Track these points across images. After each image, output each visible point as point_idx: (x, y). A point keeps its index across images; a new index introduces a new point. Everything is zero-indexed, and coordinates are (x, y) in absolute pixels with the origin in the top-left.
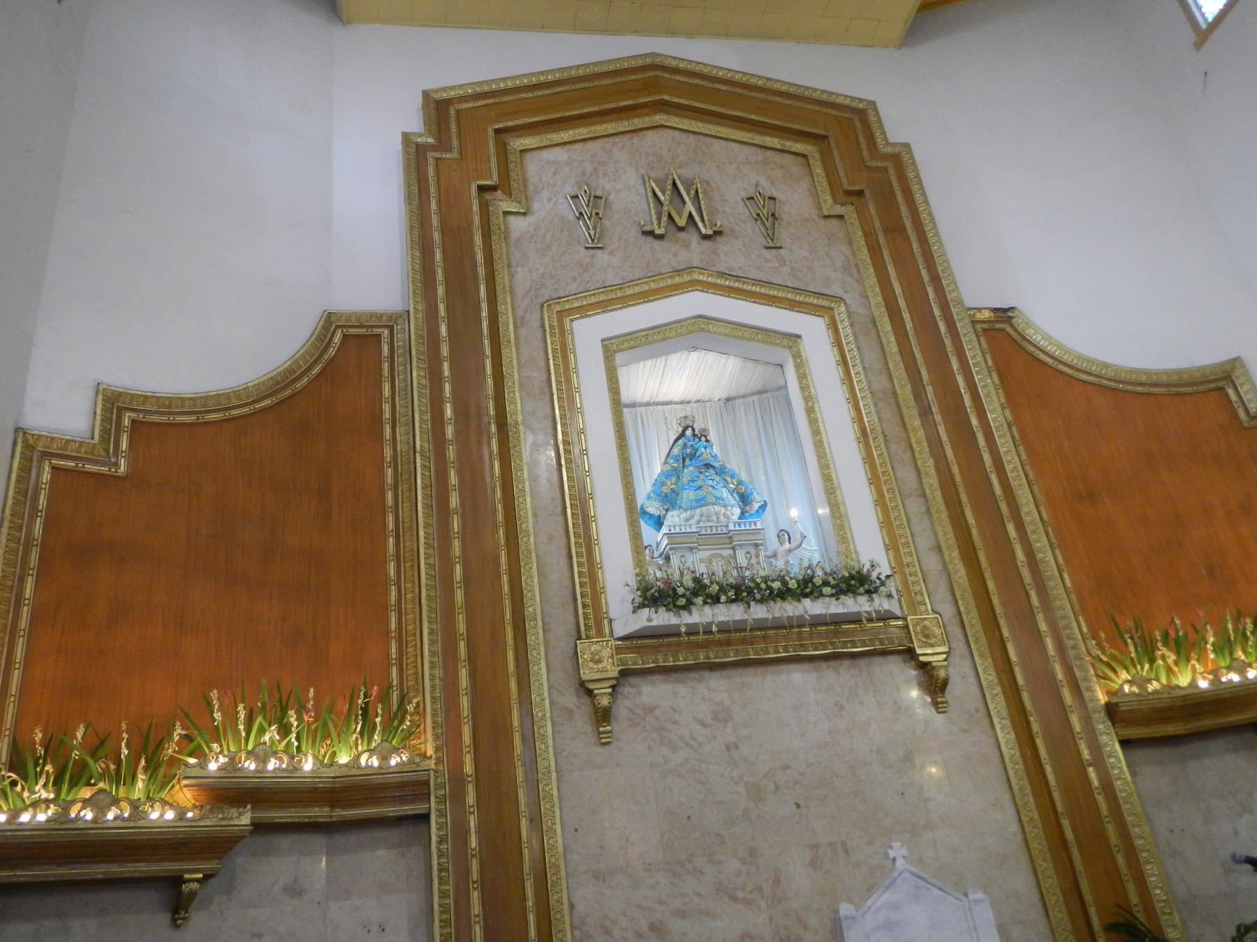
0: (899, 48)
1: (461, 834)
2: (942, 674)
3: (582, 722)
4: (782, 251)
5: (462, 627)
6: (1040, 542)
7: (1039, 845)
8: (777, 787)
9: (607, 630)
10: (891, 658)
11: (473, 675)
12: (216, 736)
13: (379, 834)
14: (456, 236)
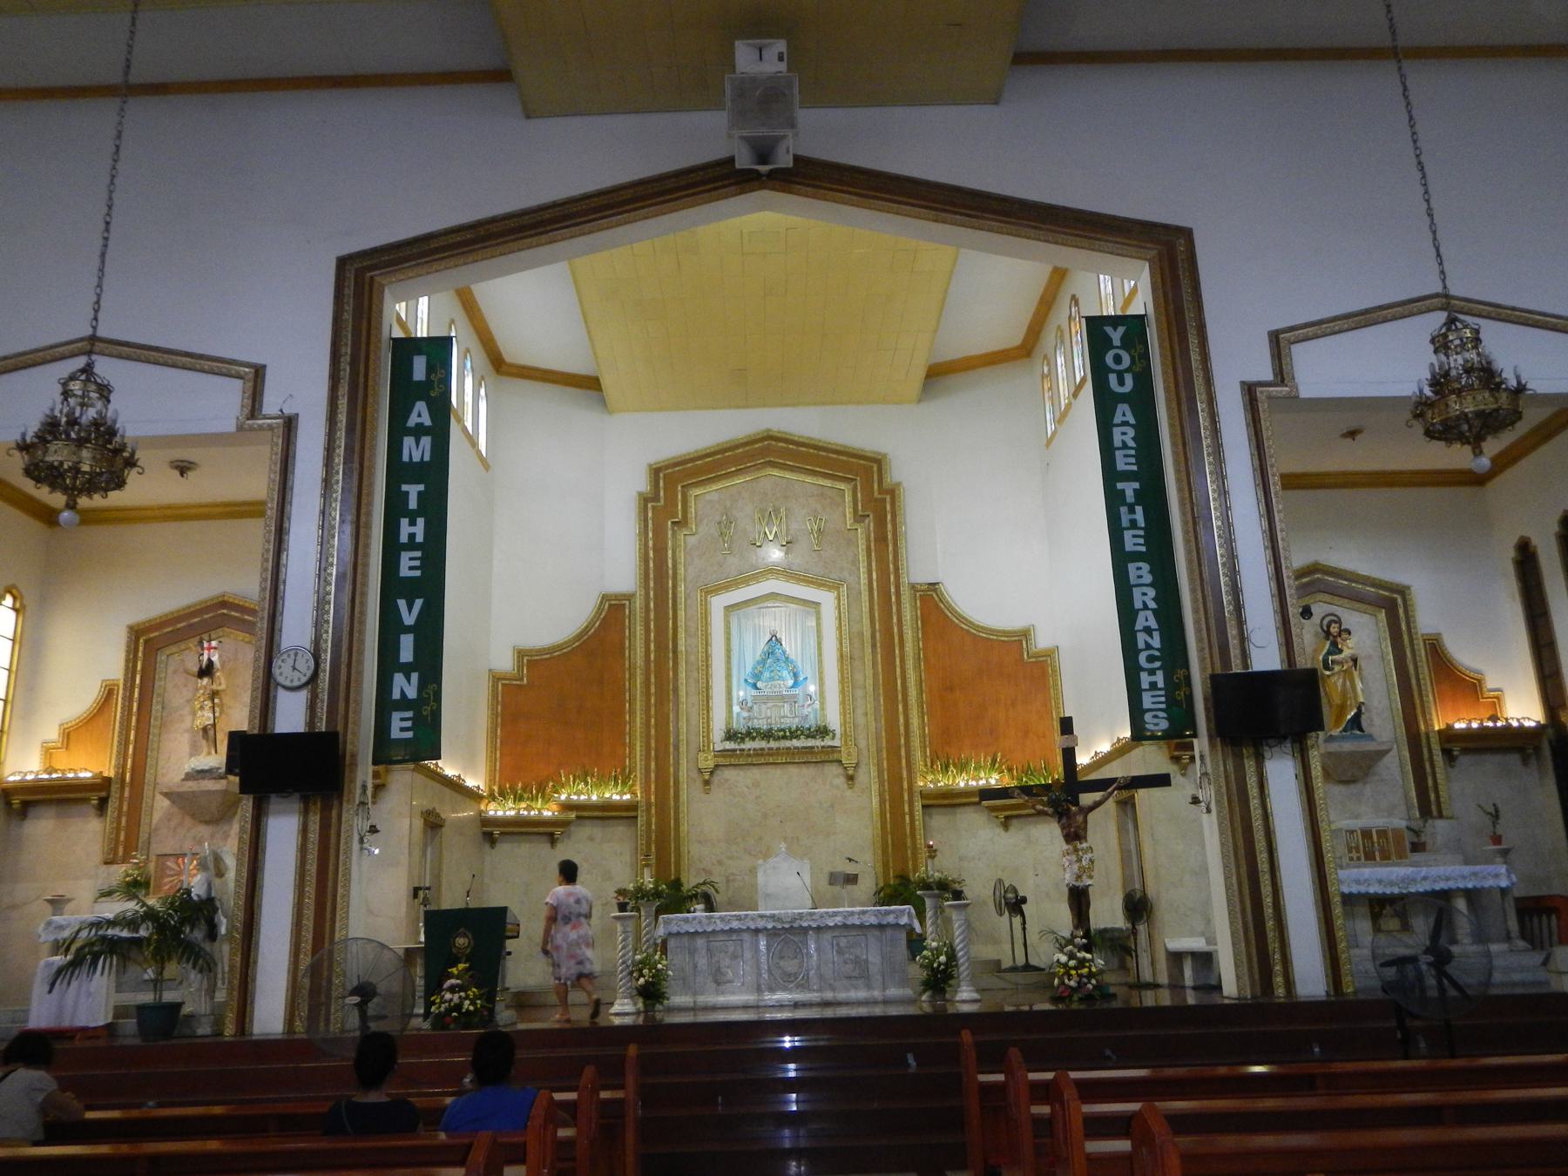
0: (920, 401)
1: (649, 824)
2: (850, 772)
3: (699, 784)
5: (653, 745)
7: (879, 844)
11: (656, 764)
12: (563, 786)
13: (620, 822)
14: (660, 550)
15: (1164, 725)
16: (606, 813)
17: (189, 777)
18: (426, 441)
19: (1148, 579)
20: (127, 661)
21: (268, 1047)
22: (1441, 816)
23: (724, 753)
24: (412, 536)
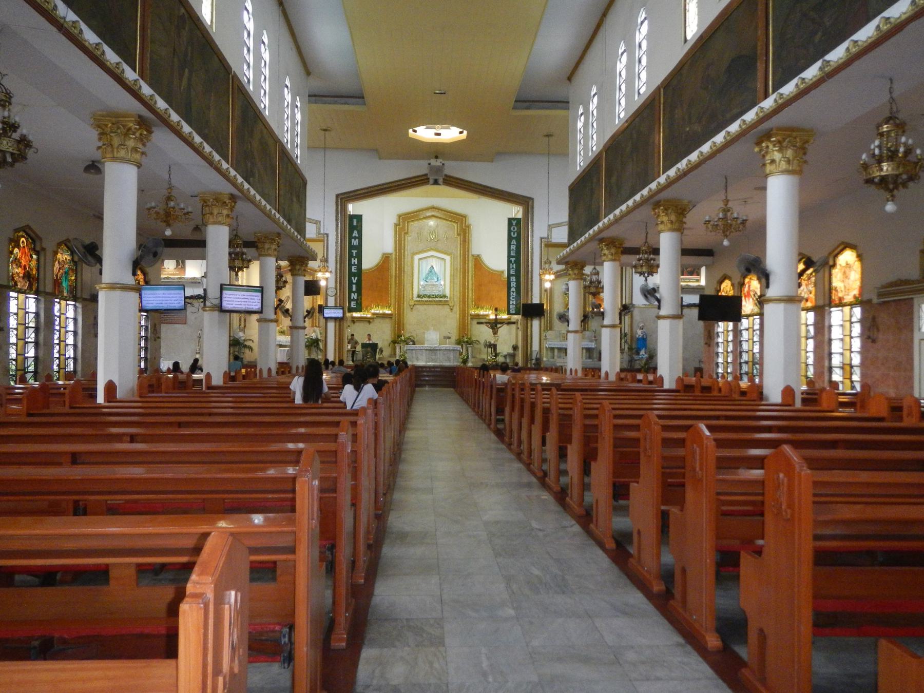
14: (400, 241)
15: (514, 312)
16: (384, 316)
18: (357, 240)
19: (515, 280)
22: (588, 330)
23: (417, 301)
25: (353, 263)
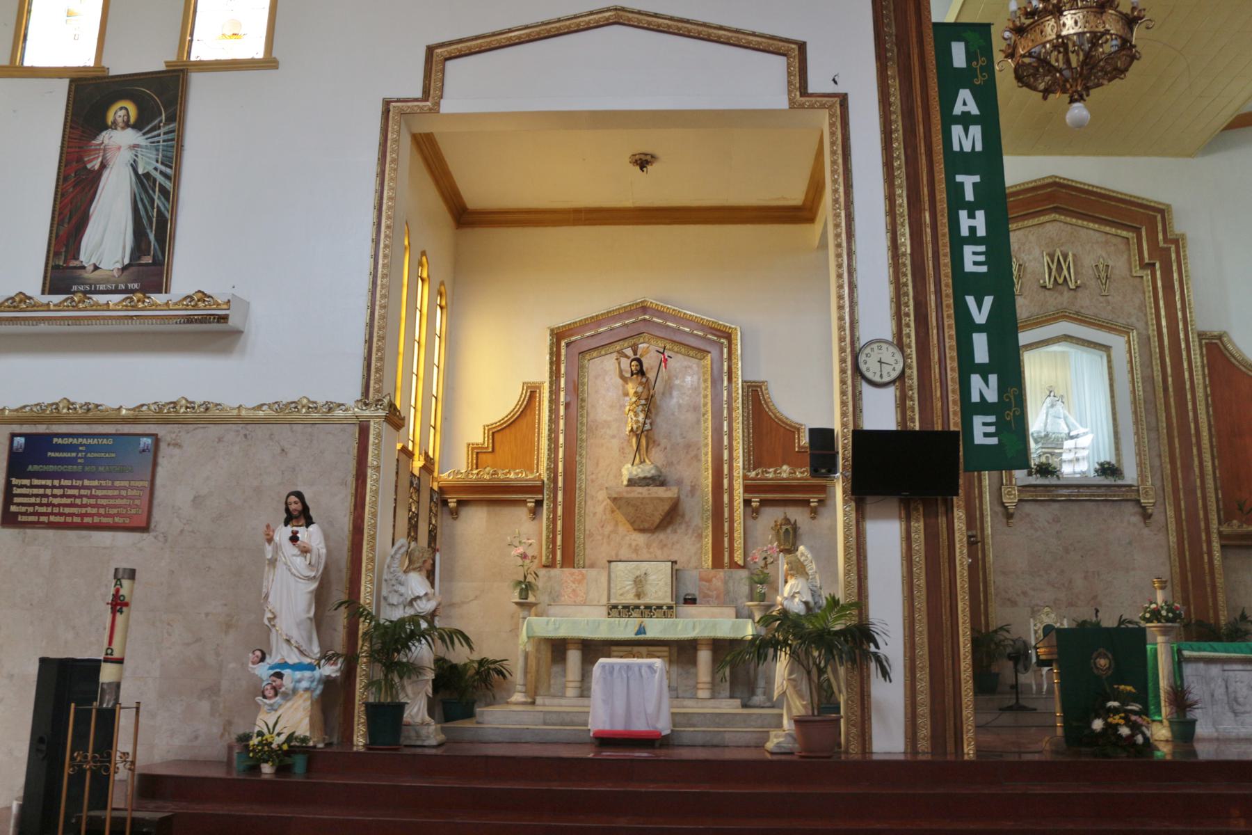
2: (1150, 511)
4: (1109, 298)
6: (1207, 457)
8: (1075, 550)
9: (1014, 483)
10: (1130, 503)
17: (632, 482)
20: (551, 363)
21: (888, 768)
24: (973, 230)
25: (965, 232)
